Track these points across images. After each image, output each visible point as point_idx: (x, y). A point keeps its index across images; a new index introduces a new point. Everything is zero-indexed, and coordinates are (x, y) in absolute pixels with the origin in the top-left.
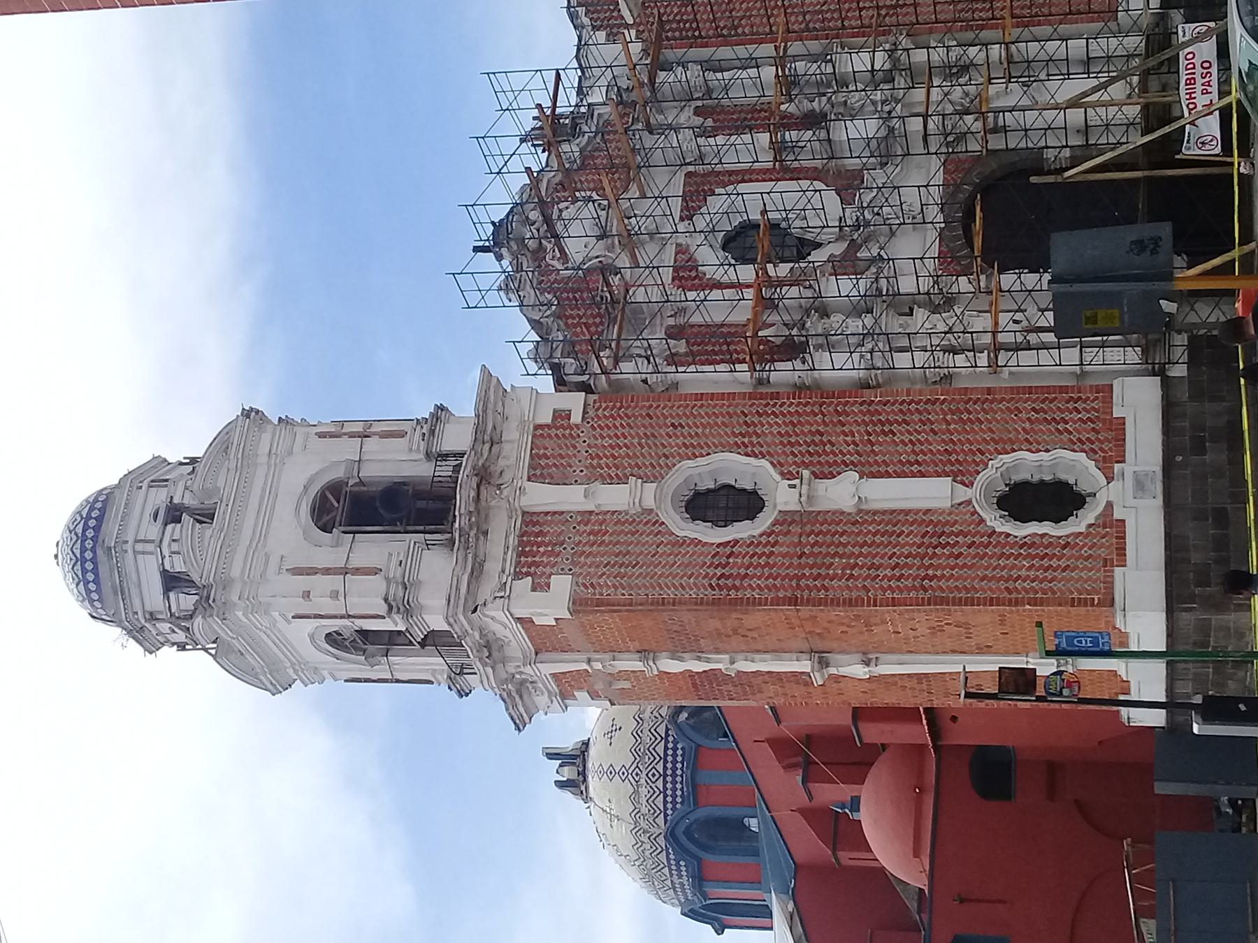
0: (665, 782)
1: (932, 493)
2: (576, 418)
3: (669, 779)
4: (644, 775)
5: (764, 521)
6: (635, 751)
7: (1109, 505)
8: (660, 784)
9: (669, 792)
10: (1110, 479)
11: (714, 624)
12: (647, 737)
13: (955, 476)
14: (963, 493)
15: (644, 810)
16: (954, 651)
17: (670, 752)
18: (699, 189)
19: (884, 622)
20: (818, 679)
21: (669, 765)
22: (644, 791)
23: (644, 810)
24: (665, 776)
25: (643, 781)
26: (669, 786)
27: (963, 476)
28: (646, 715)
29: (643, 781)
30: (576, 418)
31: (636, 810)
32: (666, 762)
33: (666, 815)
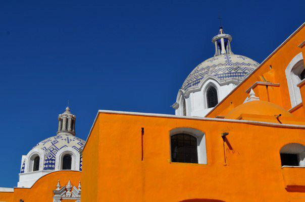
0: (228, 73)
3: (229, 75)
4: (229, 66)
6: (237, 63)
9: (224, 75)
12: (243, 67)
17: (239, 74)
21: (234, 74)
24: (230, 73)
25: (227, 66)
26: (227, 75)
28: (250, 66)
29: (227, 66)
31: (215, 66)
32: (236, 73)
33: (215, 75)
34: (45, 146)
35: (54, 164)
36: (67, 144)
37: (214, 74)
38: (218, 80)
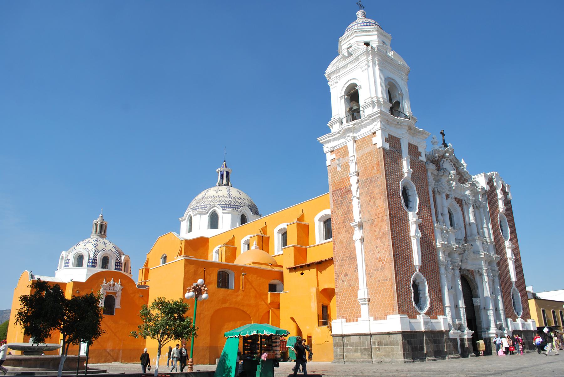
1: (417, 260)
2: (420, 158)
5: (405, 208)
6: (235, 198)
7: (420, 314)
8: (228, 203)
10: (425, 314)
11: (377, 191)
12: (239, 201)
13: (421, 267)
14: (418, 270)
15: (220, 199)
16: (367, 266)
18: (460, 202)
19: (383, 243)
20: (352, 224)
22: (226, 199)
23: (220, 199)
27: (422, 269)
28: (245, 201)
30: (420, 158)
31: (219, 197)
34: (87, 246)
35: (96, 263)
36: (105, 248)
37: (218, 203)
38: (221, 209)
